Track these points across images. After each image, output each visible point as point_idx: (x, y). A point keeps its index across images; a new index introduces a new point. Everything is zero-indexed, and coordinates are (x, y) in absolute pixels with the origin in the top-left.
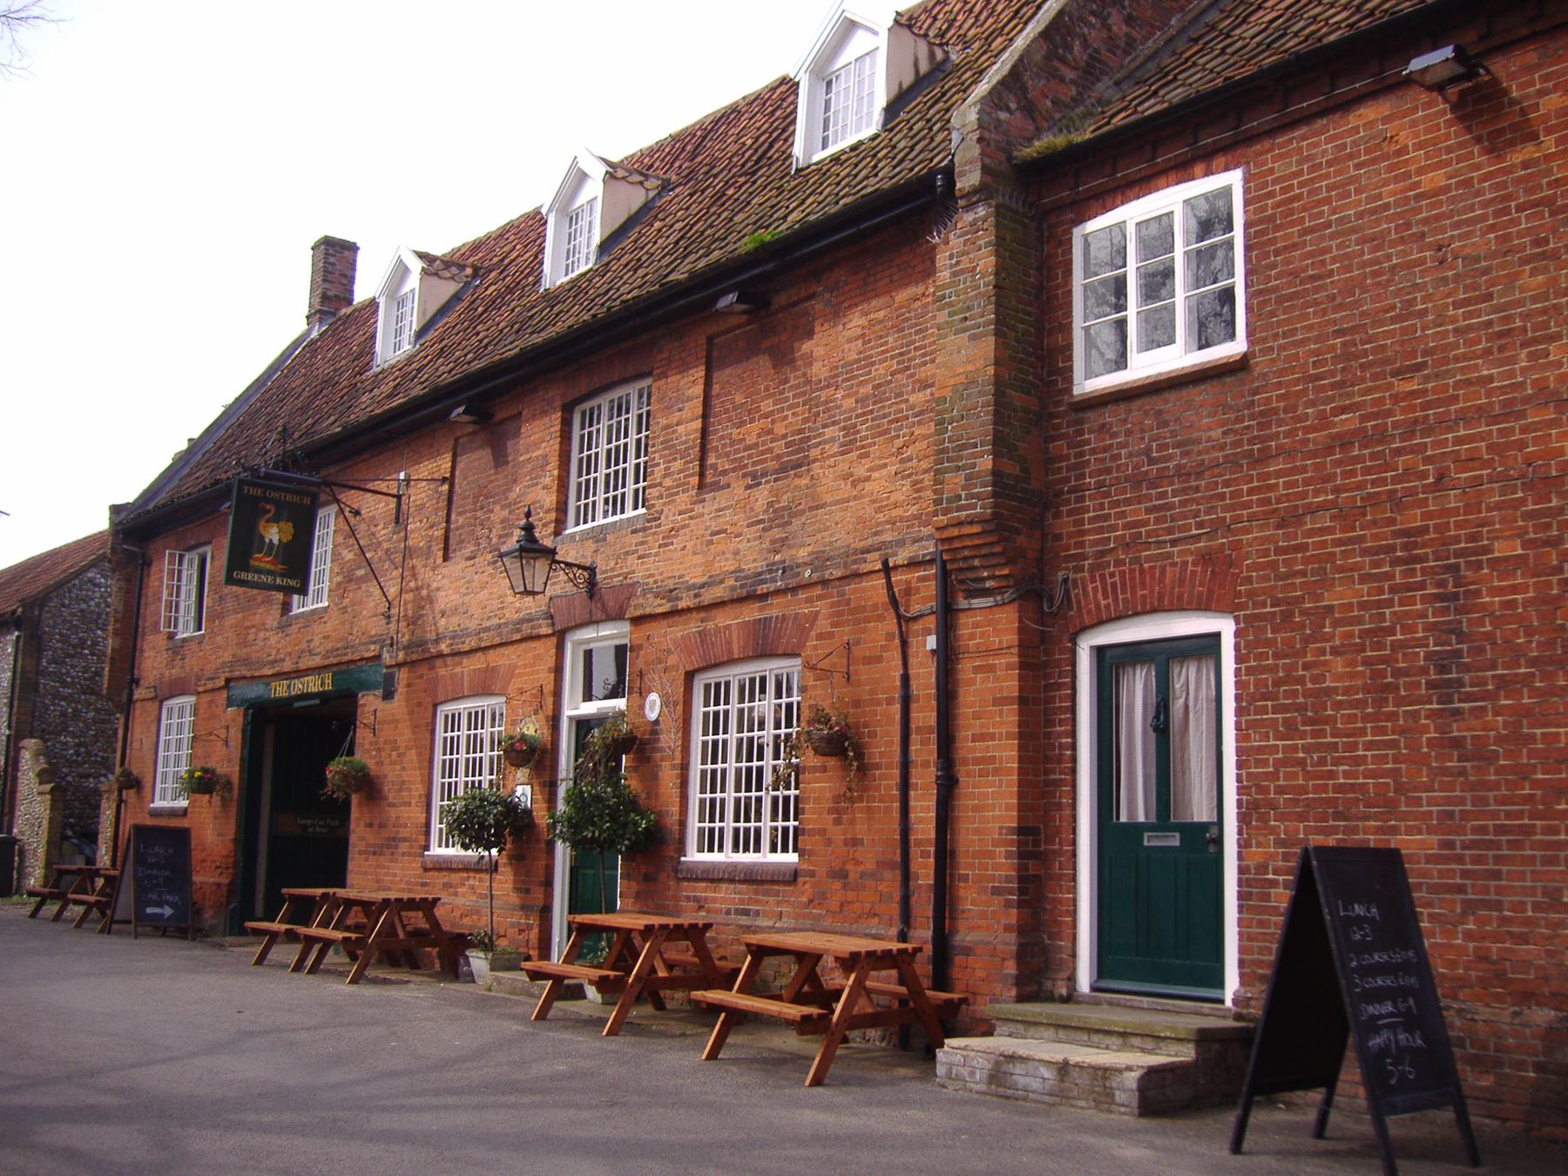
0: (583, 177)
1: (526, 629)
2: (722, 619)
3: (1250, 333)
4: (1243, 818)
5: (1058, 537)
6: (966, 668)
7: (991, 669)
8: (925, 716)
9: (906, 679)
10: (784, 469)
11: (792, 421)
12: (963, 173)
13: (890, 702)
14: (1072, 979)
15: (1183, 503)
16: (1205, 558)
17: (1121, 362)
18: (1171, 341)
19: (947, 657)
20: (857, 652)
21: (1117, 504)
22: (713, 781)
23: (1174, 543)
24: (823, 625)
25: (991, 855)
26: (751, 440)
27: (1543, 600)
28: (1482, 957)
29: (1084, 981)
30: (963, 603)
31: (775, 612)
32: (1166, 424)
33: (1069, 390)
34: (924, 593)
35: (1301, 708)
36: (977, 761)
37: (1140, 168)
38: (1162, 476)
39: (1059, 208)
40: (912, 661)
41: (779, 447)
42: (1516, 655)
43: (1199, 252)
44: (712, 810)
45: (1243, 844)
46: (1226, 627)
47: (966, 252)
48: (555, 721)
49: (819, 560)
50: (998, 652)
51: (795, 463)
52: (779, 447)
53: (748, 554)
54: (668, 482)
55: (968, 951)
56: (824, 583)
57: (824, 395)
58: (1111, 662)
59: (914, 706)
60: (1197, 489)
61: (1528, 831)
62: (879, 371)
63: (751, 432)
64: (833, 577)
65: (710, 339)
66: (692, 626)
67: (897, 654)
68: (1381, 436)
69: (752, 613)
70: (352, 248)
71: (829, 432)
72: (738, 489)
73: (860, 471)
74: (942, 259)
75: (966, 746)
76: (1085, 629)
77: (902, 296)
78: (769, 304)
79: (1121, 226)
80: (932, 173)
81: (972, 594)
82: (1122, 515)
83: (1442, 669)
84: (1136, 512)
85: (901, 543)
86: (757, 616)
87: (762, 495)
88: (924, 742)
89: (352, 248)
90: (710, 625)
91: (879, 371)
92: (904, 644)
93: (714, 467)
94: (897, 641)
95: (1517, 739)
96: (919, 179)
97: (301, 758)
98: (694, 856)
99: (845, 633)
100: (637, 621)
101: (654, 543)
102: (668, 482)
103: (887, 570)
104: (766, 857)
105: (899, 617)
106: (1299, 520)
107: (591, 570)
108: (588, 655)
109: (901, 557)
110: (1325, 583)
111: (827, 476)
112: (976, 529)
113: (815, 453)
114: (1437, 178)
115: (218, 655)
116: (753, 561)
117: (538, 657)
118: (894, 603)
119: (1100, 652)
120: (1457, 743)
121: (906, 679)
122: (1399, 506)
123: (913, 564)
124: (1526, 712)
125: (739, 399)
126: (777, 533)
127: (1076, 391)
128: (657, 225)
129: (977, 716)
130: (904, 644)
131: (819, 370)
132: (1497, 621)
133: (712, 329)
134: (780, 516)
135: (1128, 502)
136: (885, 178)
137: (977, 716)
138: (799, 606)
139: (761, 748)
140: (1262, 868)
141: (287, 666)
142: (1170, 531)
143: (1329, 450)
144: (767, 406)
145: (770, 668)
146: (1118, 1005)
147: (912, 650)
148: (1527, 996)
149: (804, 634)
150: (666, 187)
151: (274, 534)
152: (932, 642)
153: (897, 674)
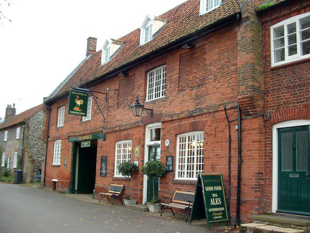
0: (149, 19)
1: (137, 124)
2: (184, 122)
5: (268, 102)
7: (252, 134)
9: (230, 136)
10: (199, 86)
12: (244, 13)
14: (271, 209)
15: (300, 93)
17: (283, 59)
19: (240, 131)
21: (283, 93)
22: (182, 160)
23: (298, 103)
24: (209, 123)
25: (251, 179)
26: (191, 79)
29: (274, 208)
30: (243, 117)
31: (197, 120)
32: (295, 74)
33: (270, 65)
34: (234, 115)
36: (248, 156)
37: (287, 12)
38: (294, 87)
39: (267, 22)
40: (231, 132)
41: (198, 81)
43: (303, 32)
44: (182, 167)
47: (244, 33)
49: (207, 108)
50: (254, 130)
52: (198, 81)
53: (190, 106)
54: (171, 89)
55: (245, 202)
59: (232, 143)
60: (303, 89)
62: (222, 62)
63: (191, 77)
65: (181, 55)
66: (176, 124)
67: (228, 130)
69: (192, 120)
72: (188, 90)
73: (218, 86)
74: (239, 34)
75: (245, 152)
77: (228, 44)
78: (195, 46)
79: (283, 27)
80: (236, 14)
82: (284, 96)
84: (287, 95)
85: (229, 103)
86: (193, 121)
87: (194, 92)
88: (235, 152)
90: (181, 123)
91: (222, 62)
93: (182, 85)
94: (228, 127)
96: (233, 15)
97: (86, 161)
98: (177, 178)
99: (214, 125)
100: (163, 122)
101: (167, 103)
102: (171, 89)
103: (225, 110)
105: (228, 121)
108: (189, 137)
109: (229, 106)
111: (211, 85)
112: (248, 99)
116: (192, 108)
117: (140, 131)
118: (227, 118)
119: (279, 129)
121: (230, 136)
123: (232, 108)
125: (188, 69)
126: (198, 101)
127: (272, 66)
128: (167, 30)
129: (248, 145)
131: (208, 62)
133: (181, 52)
134: (198, 97)
135: (286, 93)
136: (223, 16)
137: (248, 145)
138: (204, 119)
139: (194, 153)
142: (296, 100)
144: (195, 71)
145: (196, 133)
146: (283, 215)
147: (231, 129)
149: (204, 125)
150: (168, 22)
153: (228, 135)
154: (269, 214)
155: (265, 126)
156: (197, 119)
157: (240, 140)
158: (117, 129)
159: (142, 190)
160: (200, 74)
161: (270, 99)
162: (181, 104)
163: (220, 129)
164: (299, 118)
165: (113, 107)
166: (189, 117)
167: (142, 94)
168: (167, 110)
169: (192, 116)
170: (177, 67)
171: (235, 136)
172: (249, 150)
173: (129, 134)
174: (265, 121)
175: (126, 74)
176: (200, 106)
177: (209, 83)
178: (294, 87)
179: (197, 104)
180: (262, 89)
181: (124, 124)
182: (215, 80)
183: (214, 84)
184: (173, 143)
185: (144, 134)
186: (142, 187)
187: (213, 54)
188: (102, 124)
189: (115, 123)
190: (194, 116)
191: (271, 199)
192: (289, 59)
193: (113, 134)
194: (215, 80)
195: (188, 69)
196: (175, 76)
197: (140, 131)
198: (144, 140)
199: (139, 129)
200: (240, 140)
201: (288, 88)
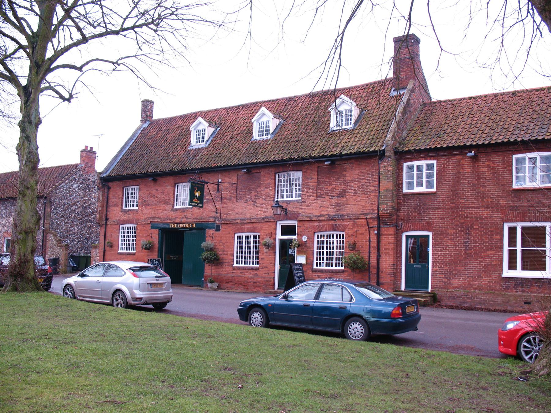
1: (266, 220)
2: (324, 223)
3: (437, 188)
4: (433, 264)
6: (382, 237)
8: (374, 244)
9: (370, 238)
11: (340, 187)
13: (366, 242)
14: (400, 287)
16: (427, 223)
18: (422, 186)
19: (379, 235)
20: (358, 232)
24: (349, 227)
26: (330, 189)
27: (481, 235)
28: (469, 284)
29: (403, 288)
30: (382, 226)
31: (338, 223)
34: (375, 223)
35: (443, 248)
38: (420, 209)
42: (476, 242)
45: (433, 268)
46: (430, 234)
47: (386, 166)
48: (275, 239)
49: (348, 214)
50: (390, 235)
51: (341, 195)
53: (331, 211)
54: (308, 194)
56: (350, 219)
57: (349, 184)
58: (407, 237)
61: (477, 267)
63: (330, 187)
64: (354, 218)
66: (316, 224)
68: (458, 208)
69: (333, 223)
70: (153, 102)
71: (350, 191)
72: (327, 198)
75: (382, 250)
76: (404, 232)
77: (367, 169)
81: (384, 225)
83: (466, 243)
84: (415, 214)
85: (369, 214)
86: (333, 223)
87: (334, 200)
89: (153, 102)
92: (369, 232)
95: (476, 254)
99: (355, 229)
100: (299, 221)
101: (304, 206)
102: (308, 194)
104: (131, 251)
106: (444, 219)
107: (286, 209)
110: (448, 229)
113: (347, 194)
114: (469, 170)
115: (146, 214)
117: (271, 226)
119: (406, 236)
120: (467, 254)
121: (370, 238)
122: (460, 219)
123: (371, 218)
124: (478, 250)
126: (338, 208)
130: (369, 232)
132: (474, 237)
134: (338, 205)
138: (345, 223)
140: (436, 271)
141: (177, 220)
143: (449, 209)
144: (334, 183)
148: (475, 289)
151: (197, 194)
152: (376, 232)
153: (368, 237)
154: (399, 291)
155: (397, 233)
156: (338, 223)
157: (379, 242)
158: (238, 221)
159: (274, 278)
160: (340, 187)
161: (401, 214)
162: (322, 207)
163: (360, 232)
164: (423, 230)
165: (230, 199)
166: (329, 220)
167: (272, 193)
168: (303, 211)
169: (332, 220)
170: (316, 177)
171: (374, 238)
172: (386, 249)
173: (255, 228)
174: (397, 229)
175: (249, 171)
176: (341, 213)
177: (349, 195)
178: (420, 209)
179: (338, 211)
180: (396, 207)
181: (248, 217)
182: (355, 195)
183: (354, 198)
184: (311, 239)
185: (276, 229)
186: (274, 275)
187: (354, 174)
188: (214, 214)
189: (233, 215)
190: (335, 220)
191: (401, 282)
192: (417, 190)
193: (231, 226)
194: (355, 195)
195: (326, 180)
196: (313, 184)
197: (271, 226)
198: (276, 234)
199: (270, 224)
200: (379, 242)
201: (415, 209)
